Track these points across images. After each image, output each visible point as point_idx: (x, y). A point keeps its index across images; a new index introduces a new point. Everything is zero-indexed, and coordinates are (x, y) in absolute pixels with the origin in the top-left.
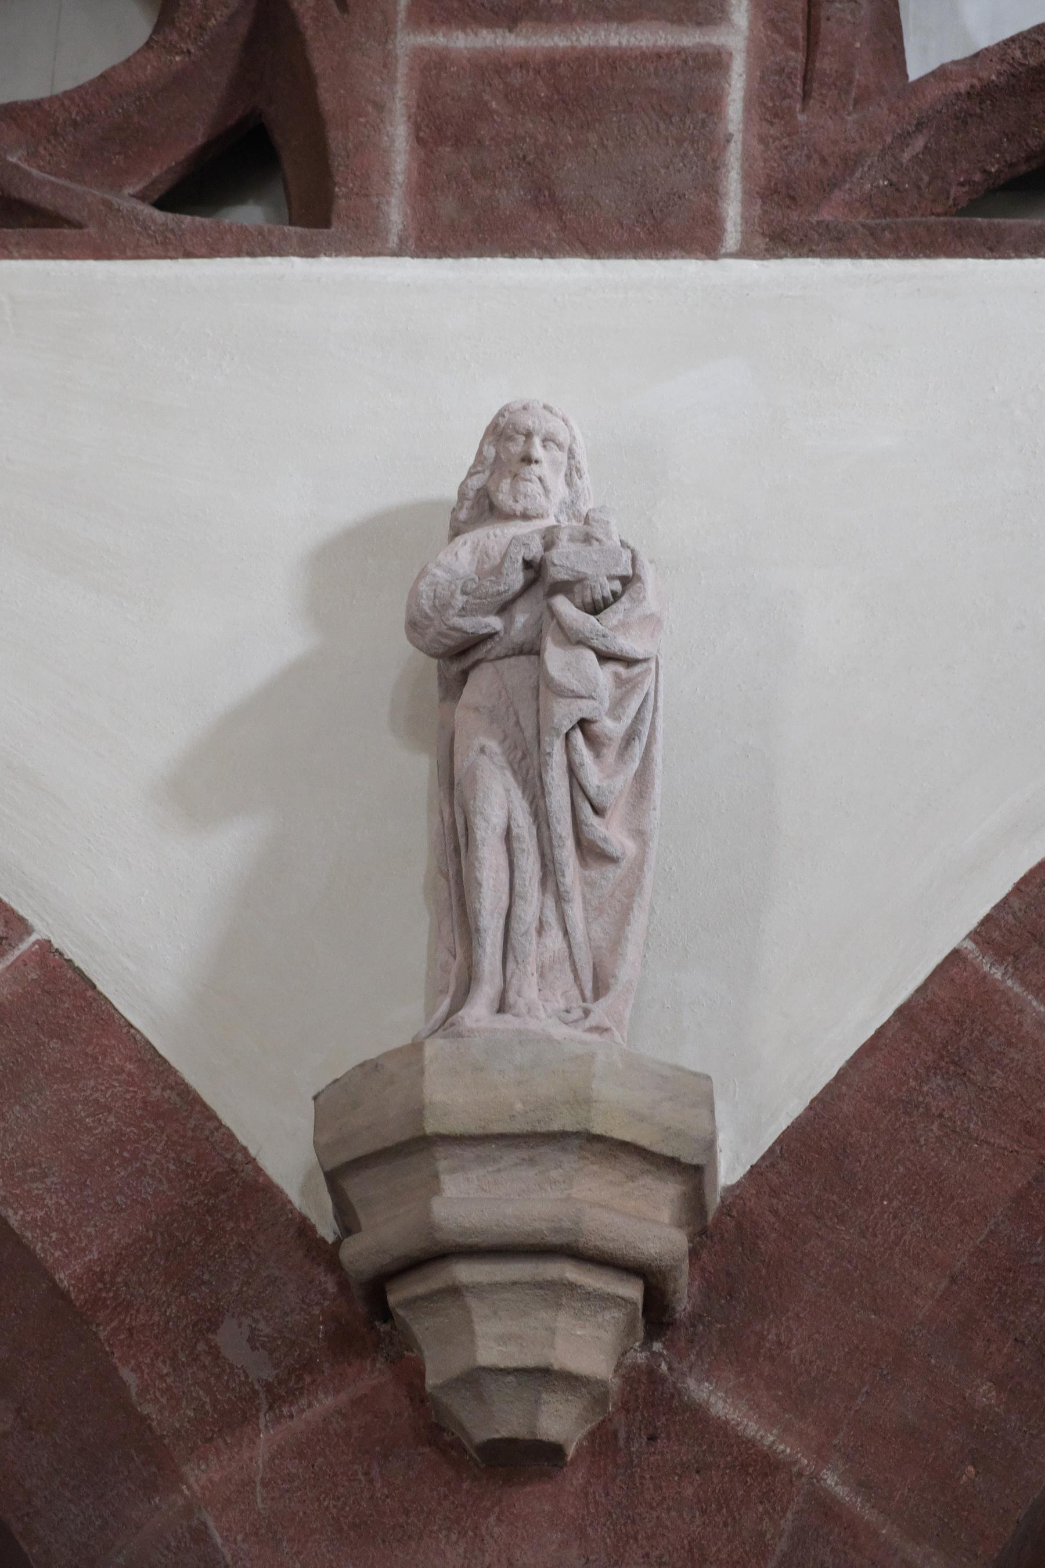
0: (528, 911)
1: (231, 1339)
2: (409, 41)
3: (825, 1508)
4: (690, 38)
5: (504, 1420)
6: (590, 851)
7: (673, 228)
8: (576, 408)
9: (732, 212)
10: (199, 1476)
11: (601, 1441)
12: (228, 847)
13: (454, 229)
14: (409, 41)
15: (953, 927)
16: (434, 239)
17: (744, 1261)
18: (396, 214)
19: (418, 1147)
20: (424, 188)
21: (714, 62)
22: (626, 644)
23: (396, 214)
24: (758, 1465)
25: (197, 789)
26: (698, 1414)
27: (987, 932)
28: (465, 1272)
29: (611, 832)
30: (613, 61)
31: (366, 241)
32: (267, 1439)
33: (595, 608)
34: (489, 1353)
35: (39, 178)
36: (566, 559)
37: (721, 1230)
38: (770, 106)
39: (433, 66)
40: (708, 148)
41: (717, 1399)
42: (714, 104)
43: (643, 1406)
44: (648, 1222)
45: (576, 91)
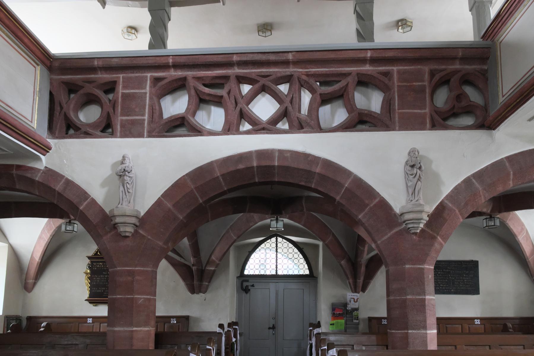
0: (124, 197)
1: (106, 228)
2: (120, 118)
3: (149, 239)
4: (143, 118)
5: (123, 234)
6: (128, 192)
7: (140, 135)
8: (130, 154)
9: (145, 134)
10: (104, 238)
11: (133, 235)
12: (105, 190)
14: (120, 118)
16: (122, 136)
17: (143, 221)
18: (118, 134)
20: (121, 132)
21: (144, 120)
22: (131, 176)
23: (118, 134)
24: (144, 236)
25: (103, 185)
26: (140, 233)
28: (119, 225)
29: (130, 191)
30: (136, 120)
31: (116, 137)
32: (109, 235)
33: (129, 173)
34: (121, 230)
35: (90, 131)
36: (126, 169)
38: (149, 124)
39: (122, 120)
40: (144, 127)
41: (141, 232)
42: (144, 124)
43: (136, 232)
44: (134, 220)
45: (133, 122)
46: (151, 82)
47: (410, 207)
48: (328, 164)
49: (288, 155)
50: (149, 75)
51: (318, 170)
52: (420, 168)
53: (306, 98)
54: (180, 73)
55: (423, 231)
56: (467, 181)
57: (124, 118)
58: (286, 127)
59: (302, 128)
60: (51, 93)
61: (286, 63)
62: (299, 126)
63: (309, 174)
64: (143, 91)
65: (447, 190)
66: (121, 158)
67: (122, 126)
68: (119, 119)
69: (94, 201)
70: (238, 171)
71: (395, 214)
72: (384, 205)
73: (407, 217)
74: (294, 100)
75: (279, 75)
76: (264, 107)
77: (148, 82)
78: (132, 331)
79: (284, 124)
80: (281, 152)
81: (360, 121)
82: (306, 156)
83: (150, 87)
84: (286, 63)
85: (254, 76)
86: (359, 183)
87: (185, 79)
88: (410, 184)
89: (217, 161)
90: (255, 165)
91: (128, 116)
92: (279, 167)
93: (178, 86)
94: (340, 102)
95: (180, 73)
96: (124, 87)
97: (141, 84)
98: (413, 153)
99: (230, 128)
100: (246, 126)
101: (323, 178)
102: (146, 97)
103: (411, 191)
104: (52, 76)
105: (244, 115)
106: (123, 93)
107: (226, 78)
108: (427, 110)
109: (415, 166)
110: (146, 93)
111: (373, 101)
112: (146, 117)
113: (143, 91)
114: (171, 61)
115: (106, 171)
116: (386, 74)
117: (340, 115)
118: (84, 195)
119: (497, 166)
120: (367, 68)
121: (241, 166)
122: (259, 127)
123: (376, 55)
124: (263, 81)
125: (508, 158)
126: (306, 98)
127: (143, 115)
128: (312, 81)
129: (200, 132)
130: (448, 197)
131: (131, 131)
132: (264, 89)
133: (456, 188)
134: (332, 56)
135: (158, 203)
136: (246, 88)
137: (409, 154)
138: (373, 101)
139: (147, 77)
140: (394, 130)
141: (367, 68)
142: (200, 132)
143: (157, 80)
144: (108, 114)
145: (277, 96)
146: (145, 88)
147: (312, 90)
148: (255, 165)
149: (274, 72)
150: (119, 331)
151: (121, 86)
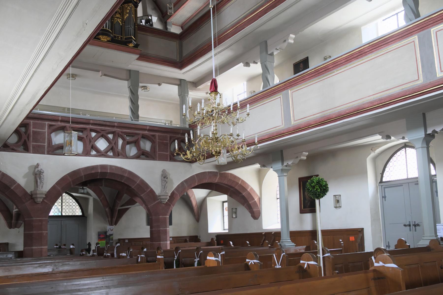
7: (43, 153)
12: (26, 179)
13: (34, 152)
14: (32, 143)
15: (54, 183)
16: (33, 153)
18: (31, 151)
19: (37, 194)
20: (33, 150)
23: (31, 151)
24: (47, 203)
25: (24, 177)
27: (56, 184)
31: (30, 153)
37: (46, 195)
38: (47, 148)
39: (33, 145)
41: (45, 201)
45: (39, 146)
46: (48, 127)
47: (163, 194)
48: (130, 173)
49: (114, 168)
50: (47, 123)
51: (126, 175)
52: (167, 178)
53: (120, 142)
54: (63, 124)
55: (167, 203)
56: (182, 183)
58: (111, 154)
59: (119, 155)
61: (114, 126)
62: (117, 155)
63: (122, 176)
65: (175, 186)
66: (35, 164)
67: (34, 147)
68: (31, 144)
69: (19, 185)
70: (92, 173)
71: (156, 195)
72: (152, 191)
73: (162, 197)
74: (116, 143)
75: (110, 131)
76: (102, 144)
77: (47, 126)
78: (42, 248)
79: (110, 153)
80: (111, 166)
81: (142, 155)
82: (121, 169)
83: (48, 129)
84: (114, 126)
85: (98, 130)
86: (143, 182)
88: (163, 184)
89: (82, 169)
90: (99, 171)
91: (36, 142)
92: (110, 173)
94: (133, 144)
95: (63, 124)
96: (33, 128)
97: (43, 127)
98: (164, 171)
99: (86, 153)
100: (94, 153)
101: (128, 179)
102: (45, 134)
103: (163, 187)
105: (94, 147)
106: (33, 131)
107: (85, 129)
108: (168, 153)
109: (165, 177)
110: (45, 132)
111: (147, 146)
112: (46, 144)
114: (60, 119)
115: (26, 170)
116: (153, 136)
117: (132, 151)
118: (13, 181)
119: (192, 177)
120: (146, 132)
121: (93, 172)
122: (100, 154)
123: (151, 128)
124: (103, 133)
125: (197, 175)
126: (120, 142)
127: (45, 143)
128: (123, 135)
130: (176, 189)
131: (38, 150)
132: (103, 136)
133: (178, 186)
134: (134, 126)
135: (54, 187)
136: (93, 134)
137: (163, 171)
138: (147, 146)
140: (156, 160)
141: (146, 132)
143: (50, 126)
144: (25, 140)
145: (107, 139)
146: (45, 129)
147: (123, 139)
150: (36, 249)
151: (32, 127)
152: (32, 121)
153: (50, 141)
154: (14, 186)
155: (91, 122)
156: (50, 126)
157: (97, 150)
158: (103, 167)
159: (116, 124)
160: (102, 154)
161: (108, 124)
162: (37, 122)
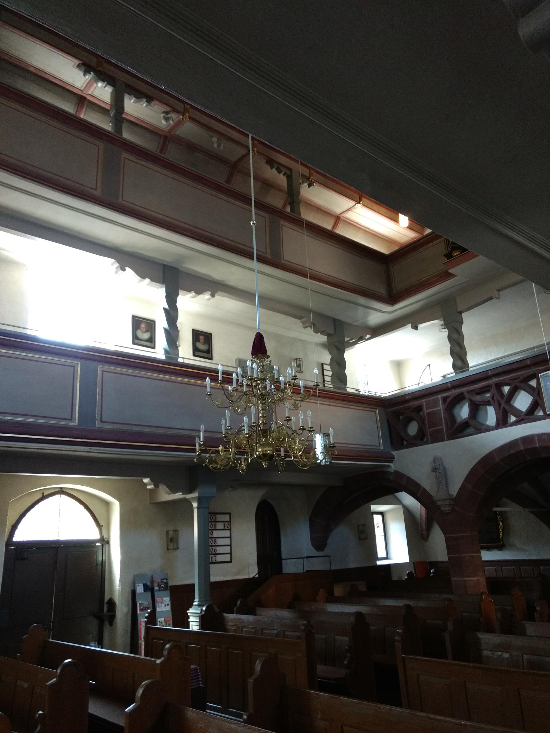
7: (443, 440)
16: (432, 443)
21: (443, 429)
38: (446, 431)
44: (448, 502)
50: (440, 396)
57: (432, 429)
60: (388, 421)
64: (439, 408)
69: (424, 489)
77: (440, 401)
78: (464, 580)
79: (539, 412)
80: (540, 436)
83: (442, 405)
87: (462, 394)
89: (495, 450)
91: (433, 427)
93: (459, 399)
97: (436, 403)
99: (502, 422)
104: (387, 410)
106: (427, 413)
110: (440, 409)
112: (444, 427)
113: (439, 408)
115: (427, 468)
121: (512, 452)
127: (442, 425)
129: (480, 430)
131: (437, 438)
139: (439, 398)
142: (480, 430)
146: (439, 406)
148: (522, 449)
149: (521, 374)
152: (424, 401)
153: (452, 418)
154: (420, 492)
155: (490, 373)
156: (444, 399)
157: (517, 413)
158: (513, 444)
159: (528, 362)
160: (522, 417)
161: (515, 366)
162: (429, 399)
